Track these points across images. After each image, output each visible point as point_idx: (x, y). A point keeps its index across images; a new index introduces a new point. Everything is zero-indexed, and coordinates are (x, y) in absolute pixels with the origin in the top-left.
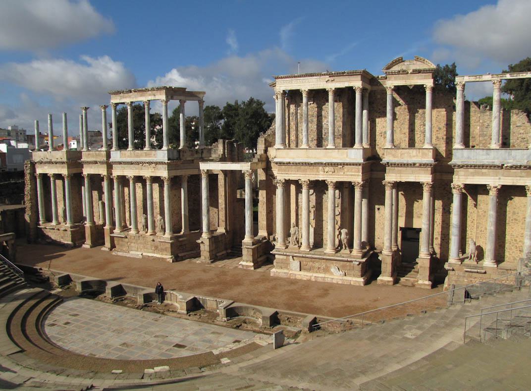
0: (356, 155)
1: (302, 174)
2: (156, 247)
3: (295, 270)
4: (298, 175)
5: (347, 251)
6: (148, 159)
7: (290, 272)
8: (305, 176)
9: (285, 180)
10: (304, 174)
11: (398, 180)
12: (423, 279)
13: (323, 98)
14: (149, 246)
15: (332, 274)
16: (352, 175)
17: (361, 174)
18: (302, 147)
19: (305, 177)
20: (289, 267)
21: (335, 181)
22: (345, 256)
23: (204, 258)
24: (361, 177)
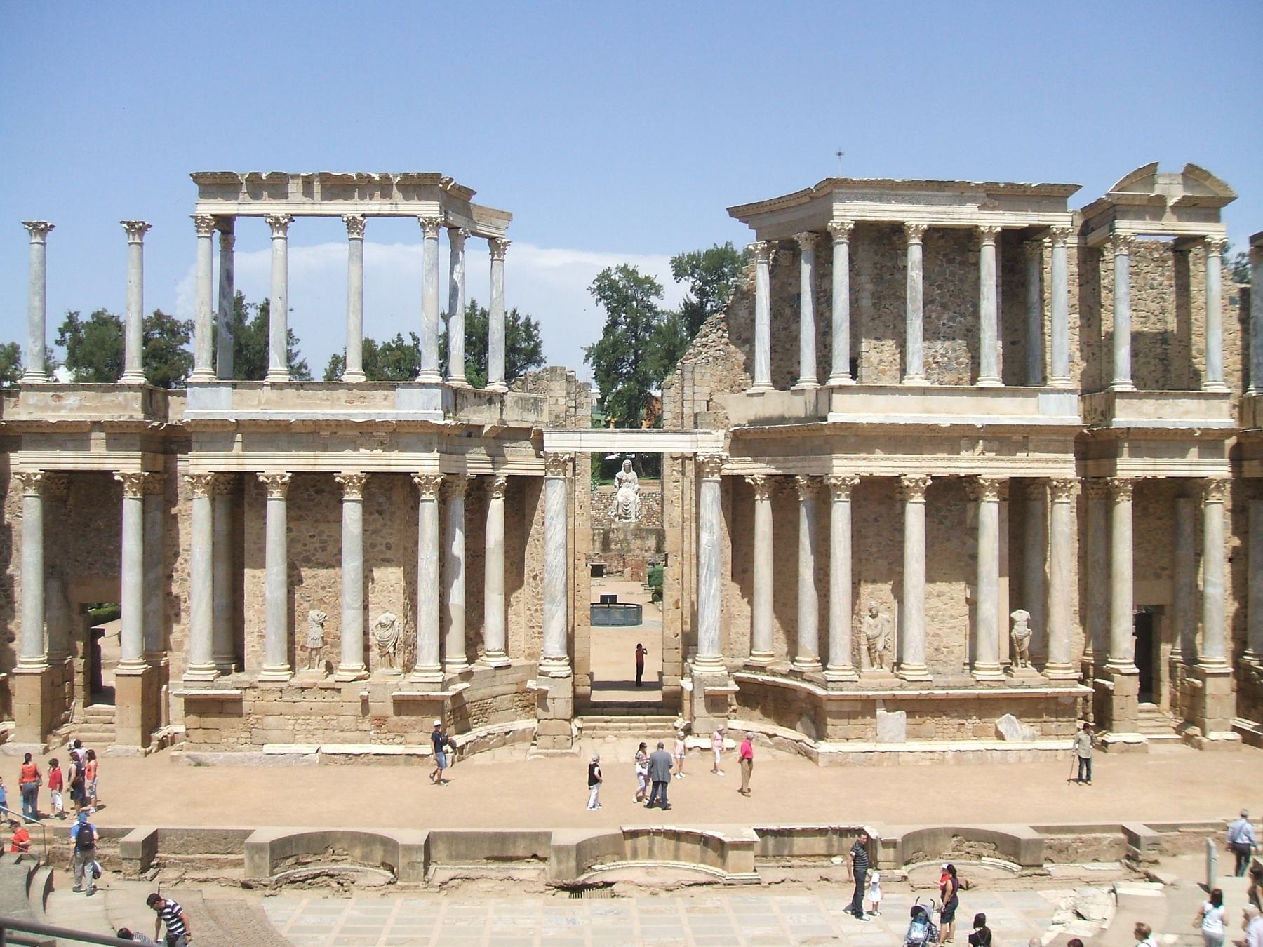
0: (1059, 408)
1: (911, 460)
2: (380, 722)
3: (892, 741)
4: (899, 463)
5: (1031, 670)
6: (359, 413)
7: (881, 747)
8: (918, 464)
9: (861, 478)
10: (918, 460)
11: (1149, 475)
12: (1219, 727)
13: (938, 253)
14: (348, 721)
15: (1000, 736)
16: (1047, 460)
17: (1071, 456)
18: (907, 383)
19: (917, 468)
20: (869, 735)
21: (1007, 474)
22: (1031, 684)
23: (550, 744)
24: (1073, 465)
